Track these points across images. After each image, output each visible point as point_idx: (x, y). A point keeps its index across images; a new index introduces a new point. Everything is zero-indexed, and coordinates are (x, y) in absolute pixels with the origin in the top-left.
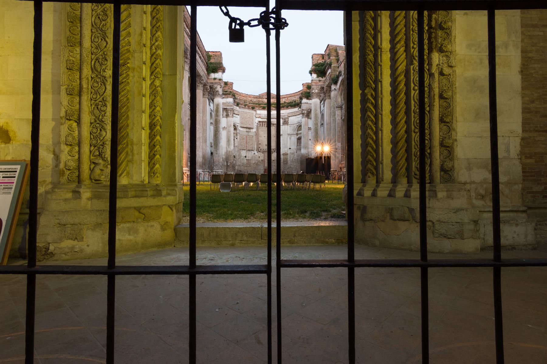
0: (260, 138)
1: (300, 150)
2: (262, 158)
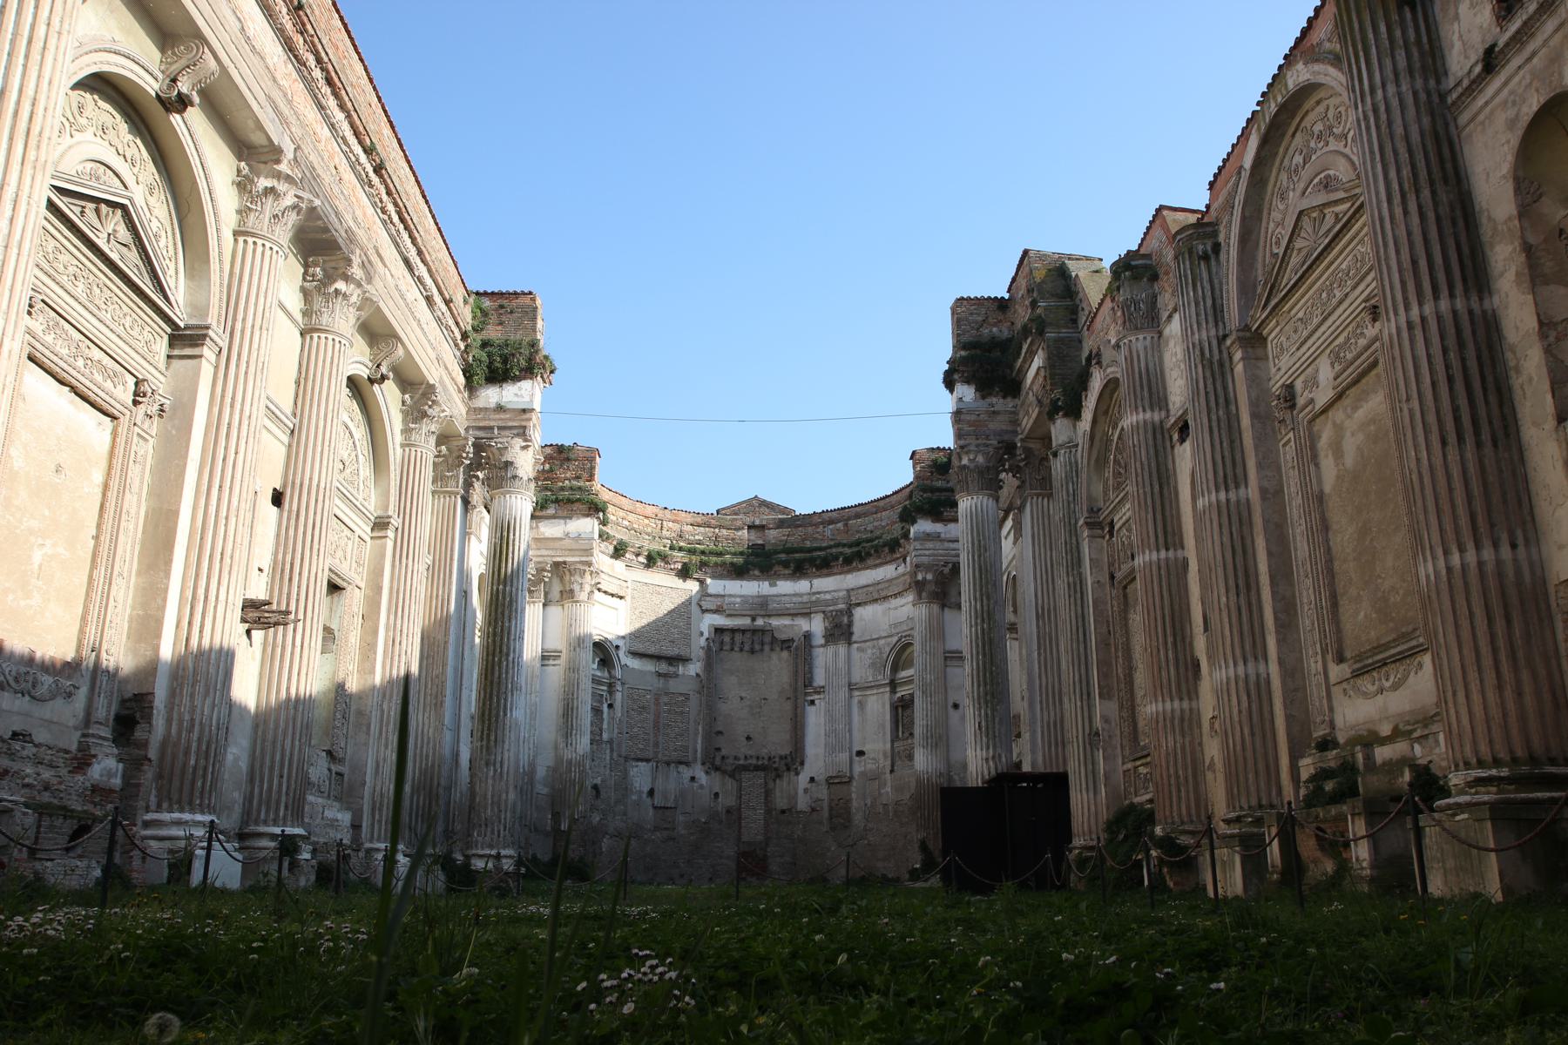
0: (724, 708)
1: (910, 757)
2: (730, 801)
